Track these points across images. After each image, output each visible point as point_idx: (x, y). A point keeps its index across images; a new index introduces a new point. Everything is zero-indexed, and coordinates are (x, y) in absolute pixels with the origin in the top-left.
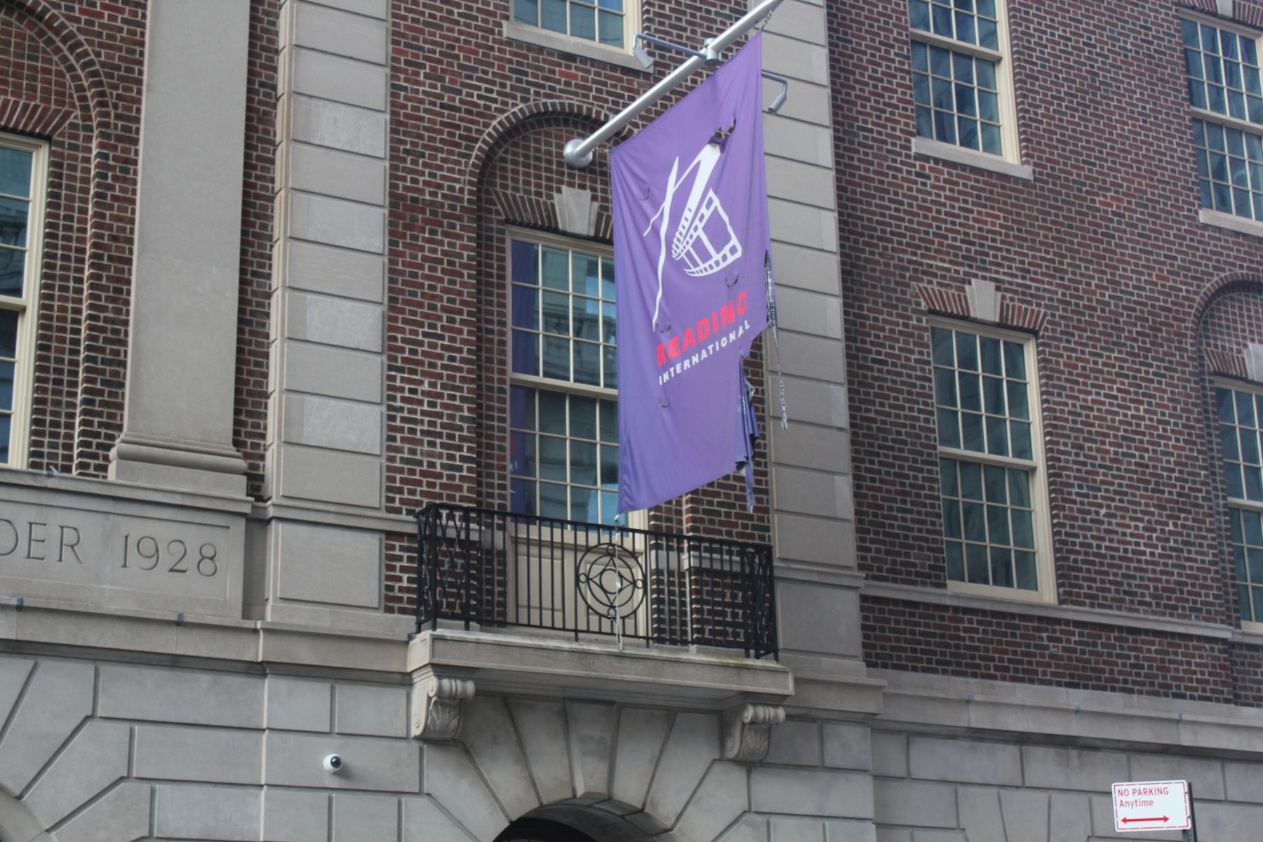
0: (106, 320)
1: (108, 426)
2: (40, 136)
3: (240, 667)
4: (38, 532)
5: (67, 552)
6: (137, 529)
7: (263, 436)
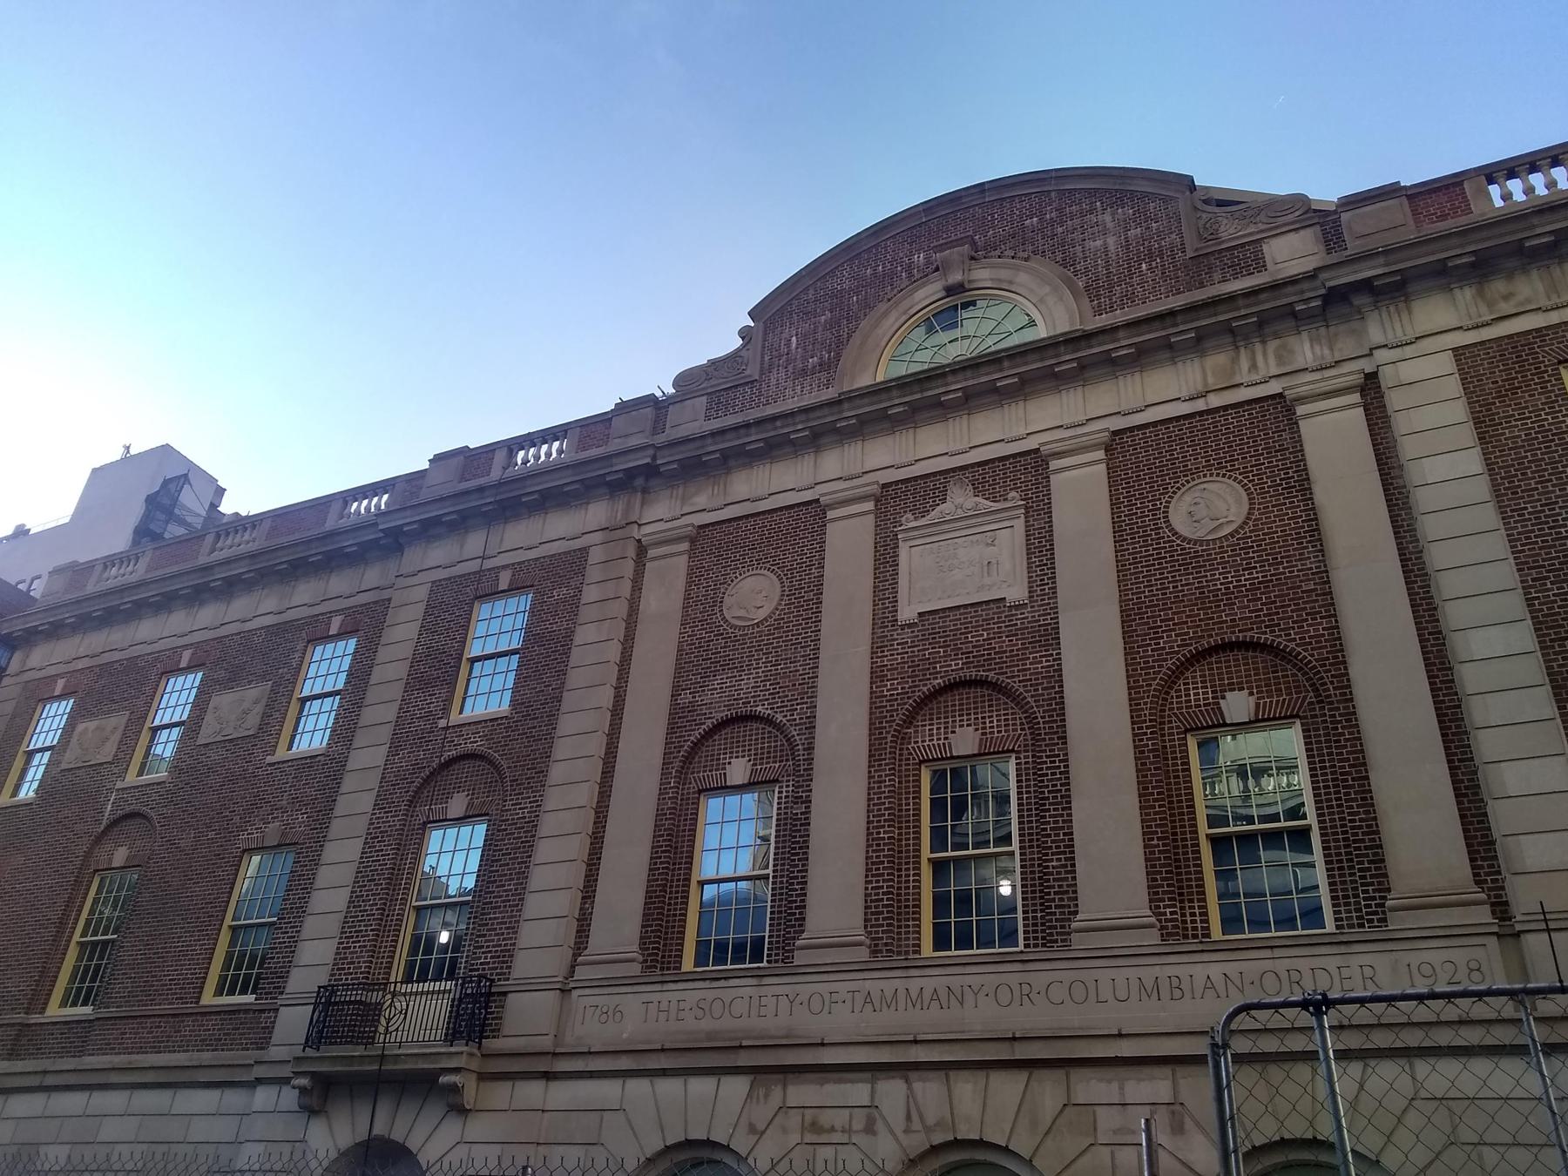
0: (1361, 820)
1: (1379, 891)
2: (1292, 716)
7: (1499, 873)
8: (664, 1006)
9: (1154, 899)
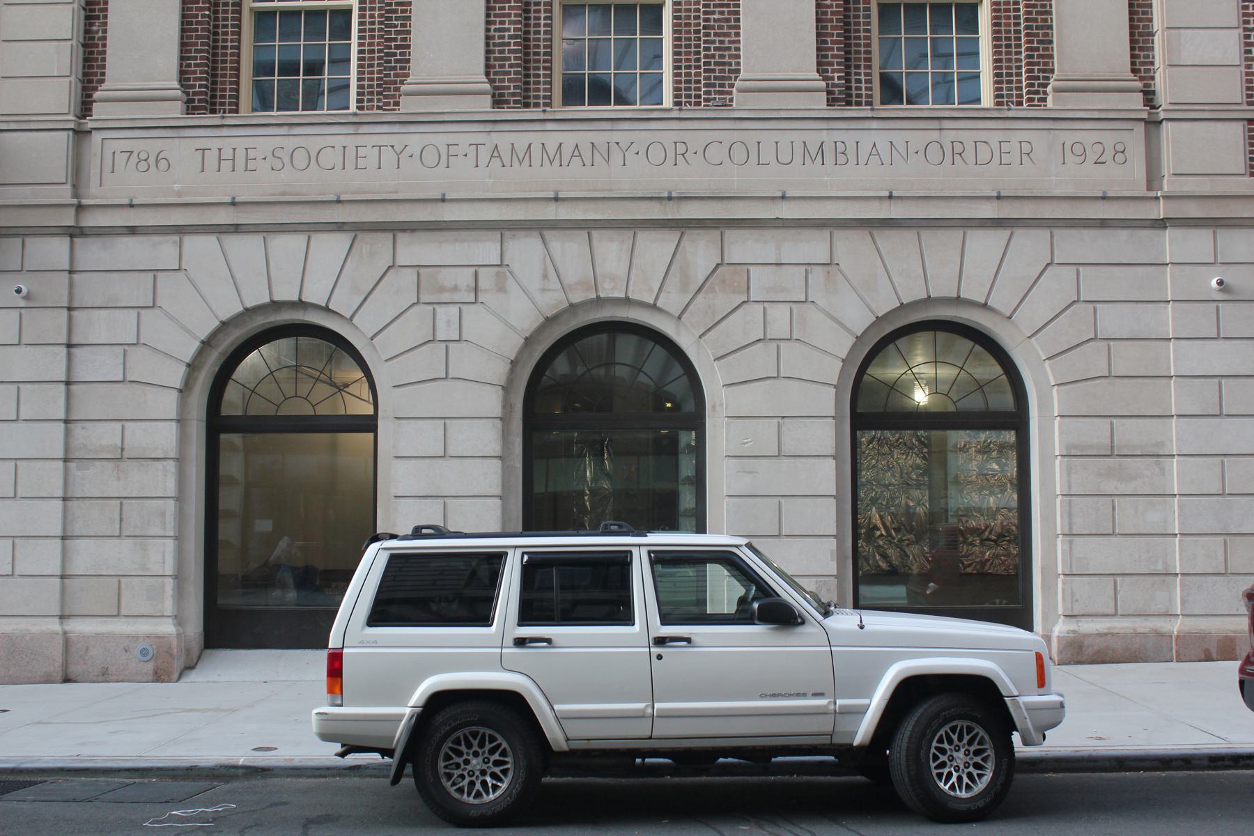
1: (1044, 71)
3: (1147, 223)
4: (1005, 147)
5: (1025, 158)
6: (1069, 138)
7: (1152, 63)
8: (227, 154)
9: (821, 65)
